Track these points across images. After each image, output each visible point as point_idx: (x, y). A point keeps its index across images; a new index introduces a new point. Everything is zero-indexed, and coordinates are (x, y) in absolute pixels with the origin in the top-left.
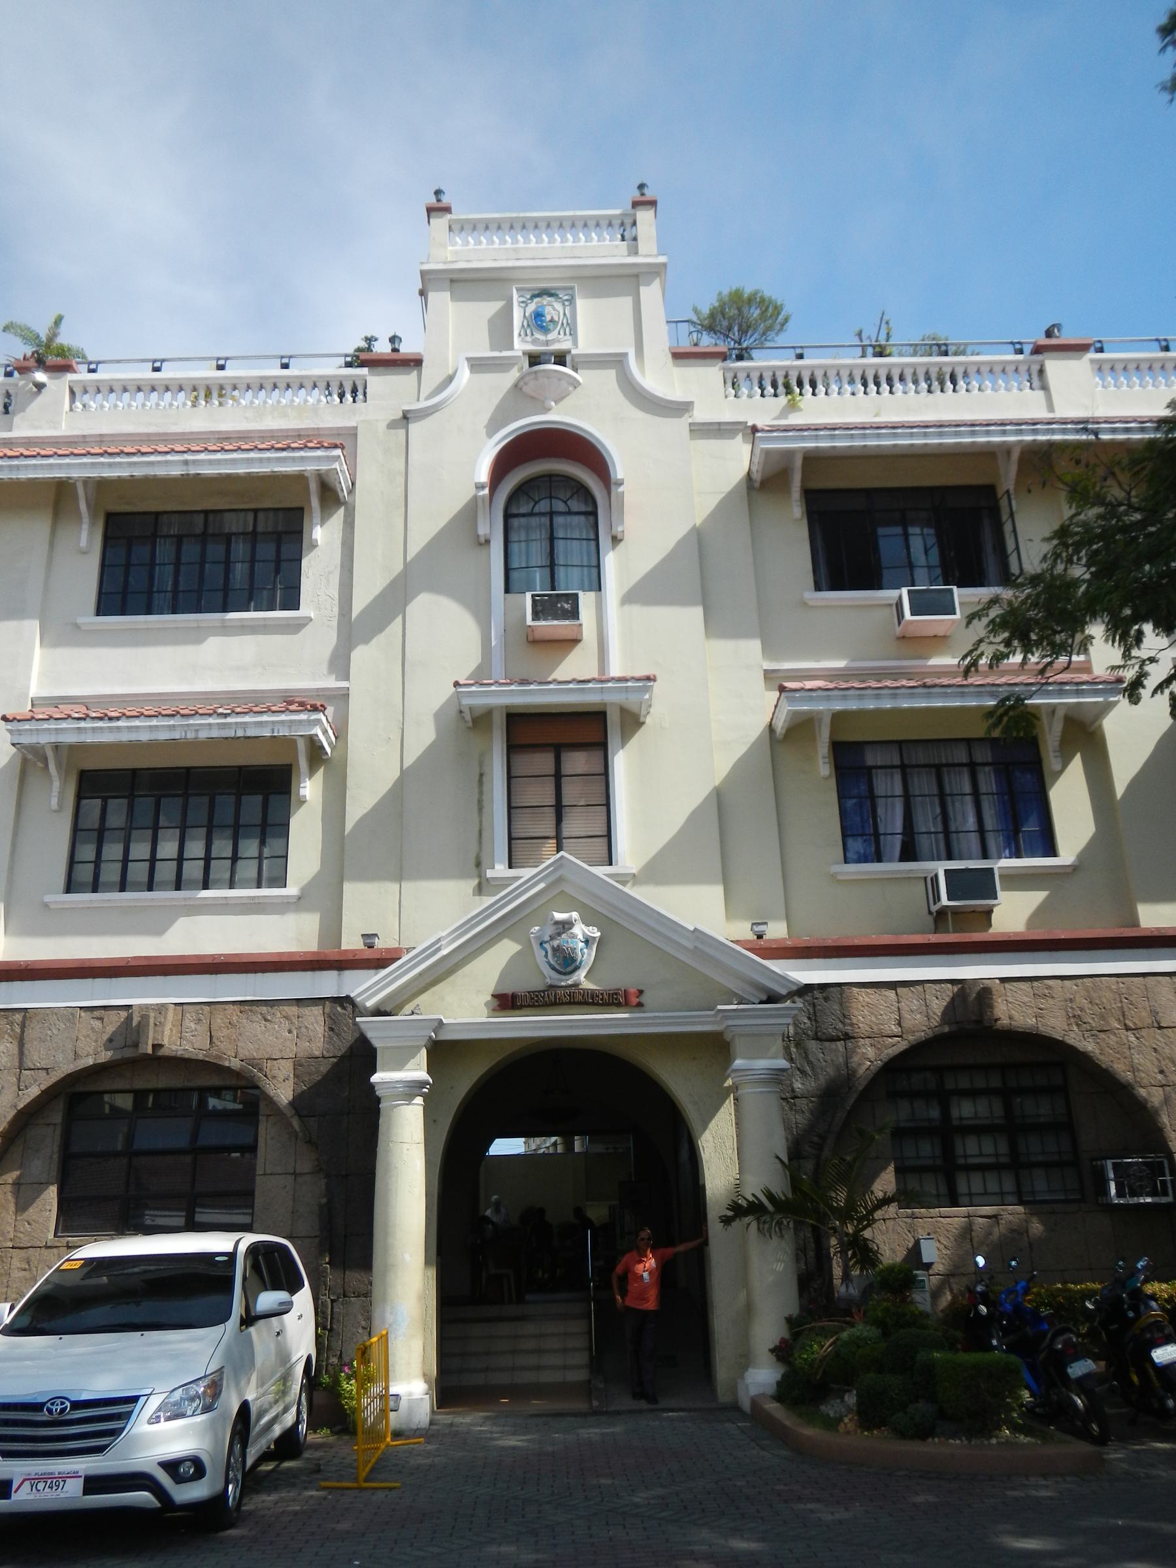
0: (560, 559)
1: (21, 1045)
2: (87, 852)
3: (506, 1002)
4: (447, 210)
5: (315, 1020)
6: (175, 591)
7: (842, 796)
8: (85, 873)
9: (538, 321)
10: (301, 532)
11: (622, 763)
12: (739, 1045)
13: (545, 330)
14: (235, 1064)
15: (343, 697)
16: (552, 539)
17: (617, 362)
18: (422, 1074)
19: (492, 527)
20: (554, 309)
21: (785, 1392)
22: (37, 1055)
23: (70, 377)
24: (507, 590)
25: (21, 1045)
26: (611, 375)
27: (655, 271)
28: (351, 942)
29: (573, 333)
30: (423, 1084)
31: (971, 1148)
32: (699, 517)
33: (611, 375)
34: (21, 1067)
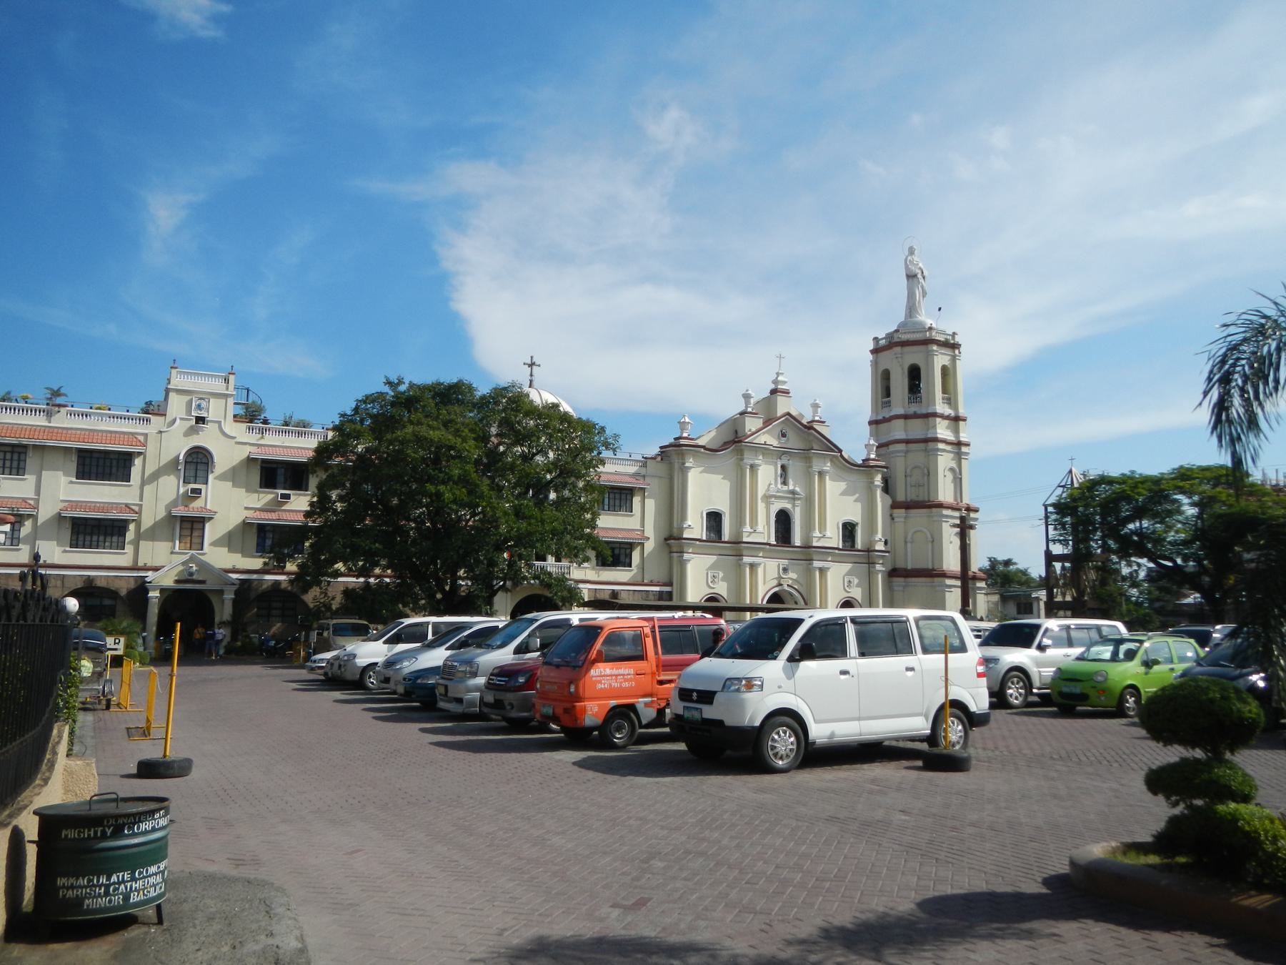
0: (198, 475)
1: (63, 582)
2: (75, 537)
3: (177, 582)
4: (176, 368)
5: (132, 580)
6: (97, 473)
7: (258, 537)
8: (74, 542)
9: (199, 407)
10: (131, 460)
11: (208, 526)
12: (225, 593)
13: (201, 410)
14: (114, 589)
15: (141, 506)
16: (196, 470)
17: (219, 423)
18: (159, 595)
19: (181, 467)
20: (204, 404)
21: (225, 653)
22: (66, 584)
23: (68, 408)
24: (184, 482)
25: (63, 582)
26: (217, 425)
27: (232, 395)
28: (140, 564)
29: (208, 412)
30: (157, 597)
31: (274, 612)
32: (234, 464)
33: (217, 425)
34: (63, 587)
